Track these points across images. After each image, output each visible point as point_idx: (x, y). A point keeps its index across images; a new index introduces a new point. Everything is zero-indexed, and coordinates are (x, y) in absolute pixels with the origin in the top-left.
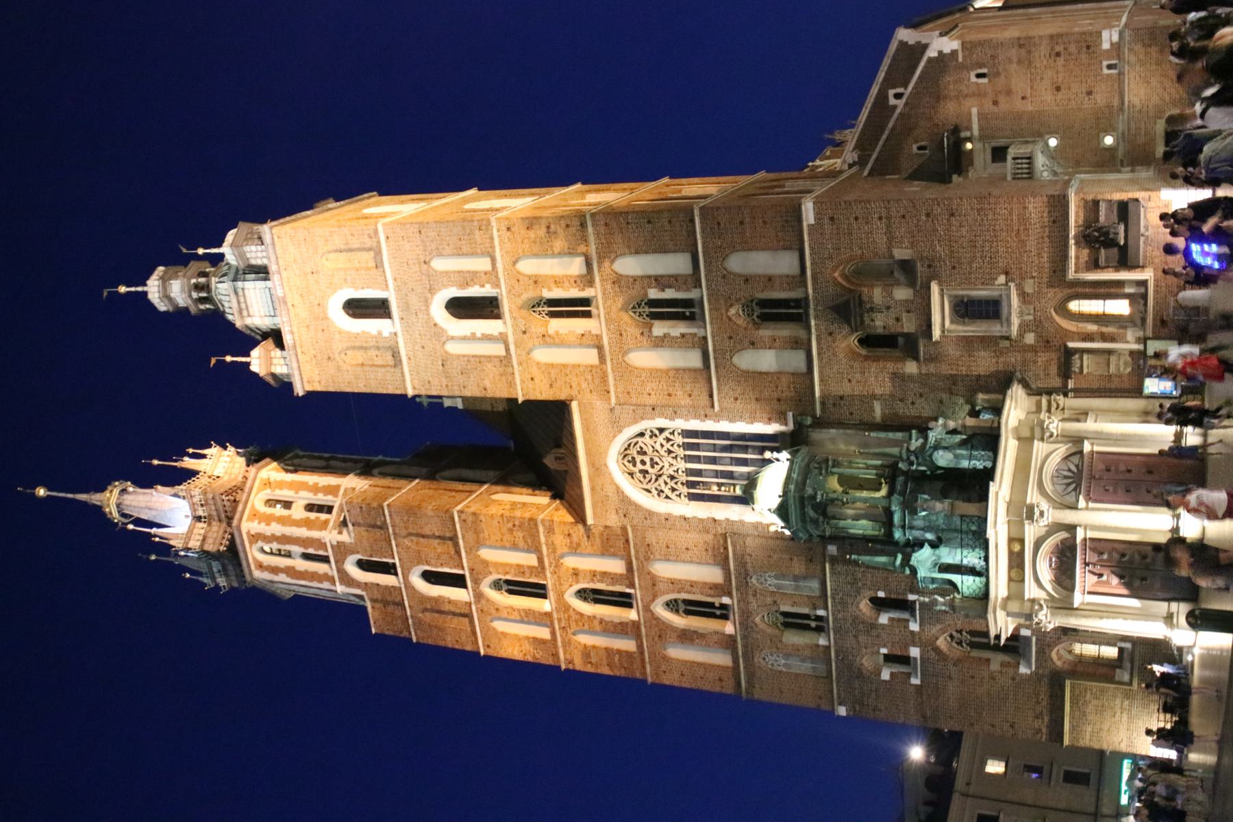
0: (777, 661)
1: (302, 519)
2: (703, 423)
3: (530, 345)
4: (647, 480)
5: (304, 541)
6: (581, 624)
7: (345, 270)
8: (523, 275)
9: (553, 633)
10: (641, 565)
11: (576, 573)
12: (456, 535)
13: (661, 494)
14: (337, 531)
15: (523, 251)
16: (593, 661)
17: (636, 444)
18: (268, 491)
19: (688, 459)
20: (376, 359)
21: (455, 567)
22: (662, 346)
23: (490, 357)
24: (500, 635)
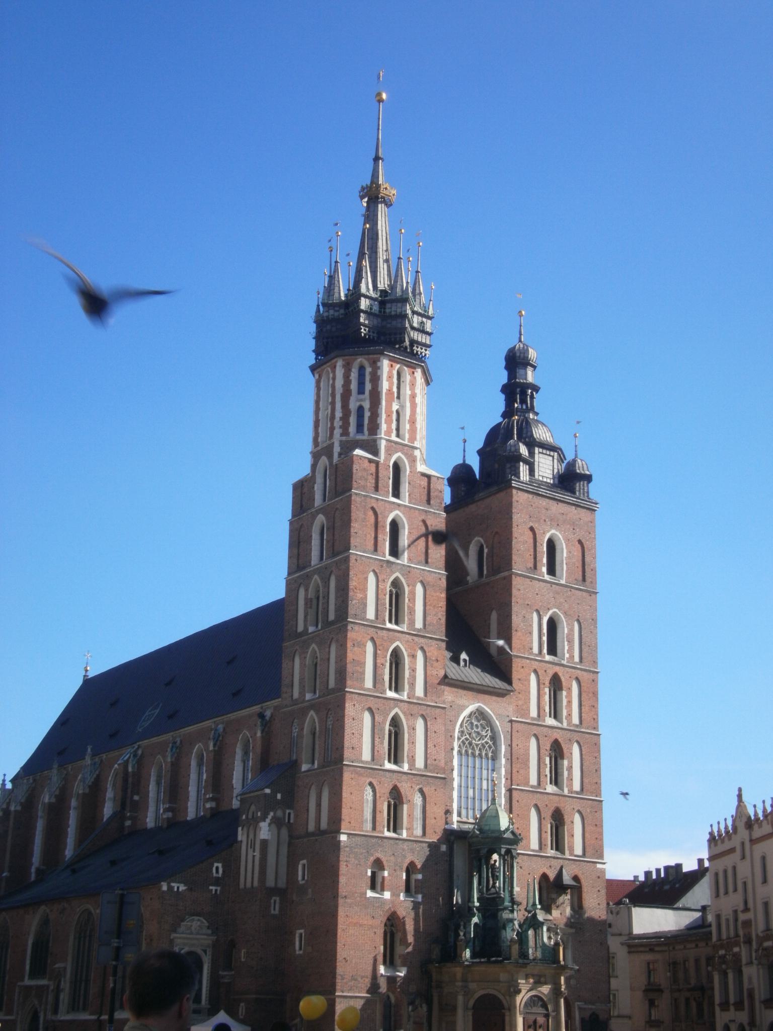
0: (369, 794)
2: (503, 777)
3: (539, 674)
5: (413, 423)
6: (381, 648)
9: (371, 621)
11: (414, 656)
15: (583, 686)
16: (356, 649)
20: (529, 554)
24: (365, 576)
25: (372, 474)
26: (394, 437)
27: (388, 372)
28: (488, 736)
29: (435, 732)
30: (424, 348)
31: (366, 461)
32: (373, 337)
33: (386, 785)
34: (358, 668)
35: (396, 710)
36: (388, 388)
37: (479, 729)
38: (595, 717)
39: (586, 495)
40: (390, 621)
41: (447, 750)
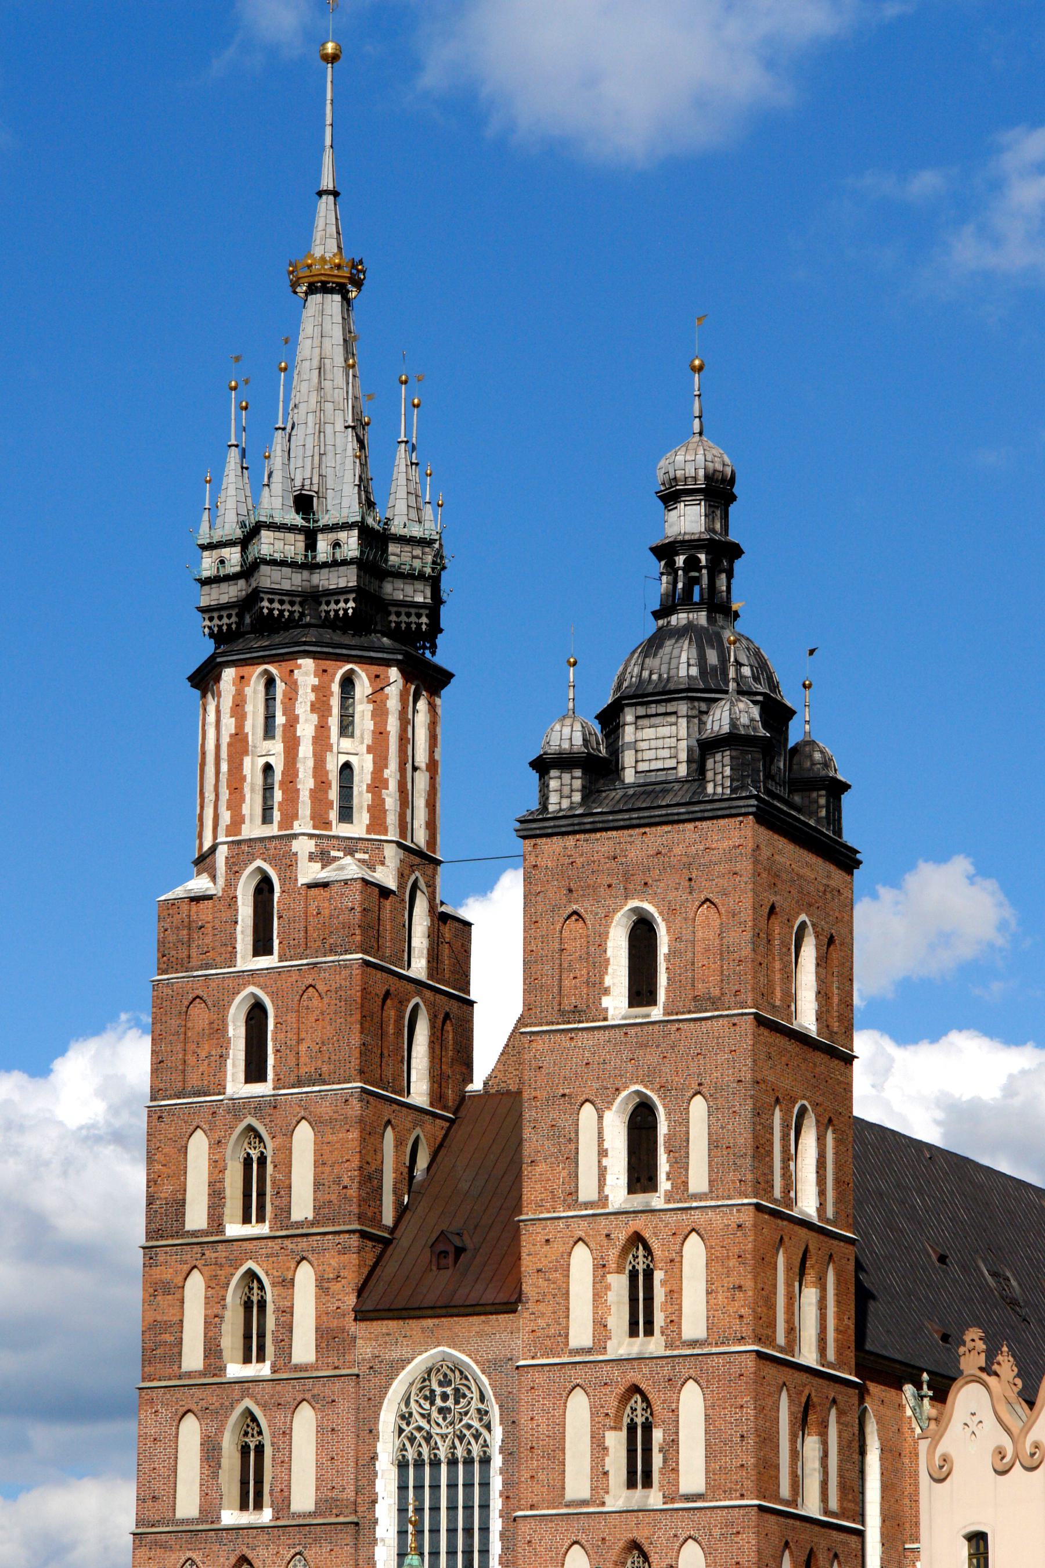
1: (327, 773)
2: (497, 1494)
3: (592, 1245)
4: (422, 1402)
7: (693, 943)
8: (683, 1244)
9: (194, 1234)
10: (307, 1387)
11: (287, 1284)
12: (325, 1083)
13: (404, 1423)
14: (313, 851)
17: (469, 1389)
18: (370, 692)
19: (453, 1462)
21: (276, 1074)
22: (592, 1443)
23: (577, 1176)
25: (201, 927)
26: (253, 829)
27: (234, 697)
28: (473, 1412)
29: (333, 1430)
30: (342, 598)
31: (185, 907)
32: (229, 625)
33: (222, 1560)
34: (168, 1338)
35: (248, 1403)
36: (233, 732)
37: (450, 1403)
38: (742, 1311)
39: (728, 783)
40: (246, 1220)
41: (361, 1462)
